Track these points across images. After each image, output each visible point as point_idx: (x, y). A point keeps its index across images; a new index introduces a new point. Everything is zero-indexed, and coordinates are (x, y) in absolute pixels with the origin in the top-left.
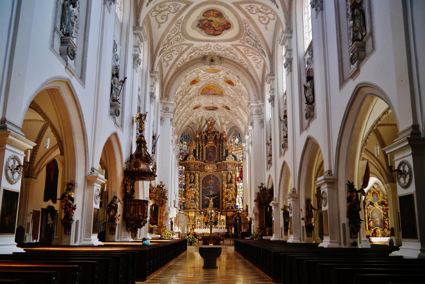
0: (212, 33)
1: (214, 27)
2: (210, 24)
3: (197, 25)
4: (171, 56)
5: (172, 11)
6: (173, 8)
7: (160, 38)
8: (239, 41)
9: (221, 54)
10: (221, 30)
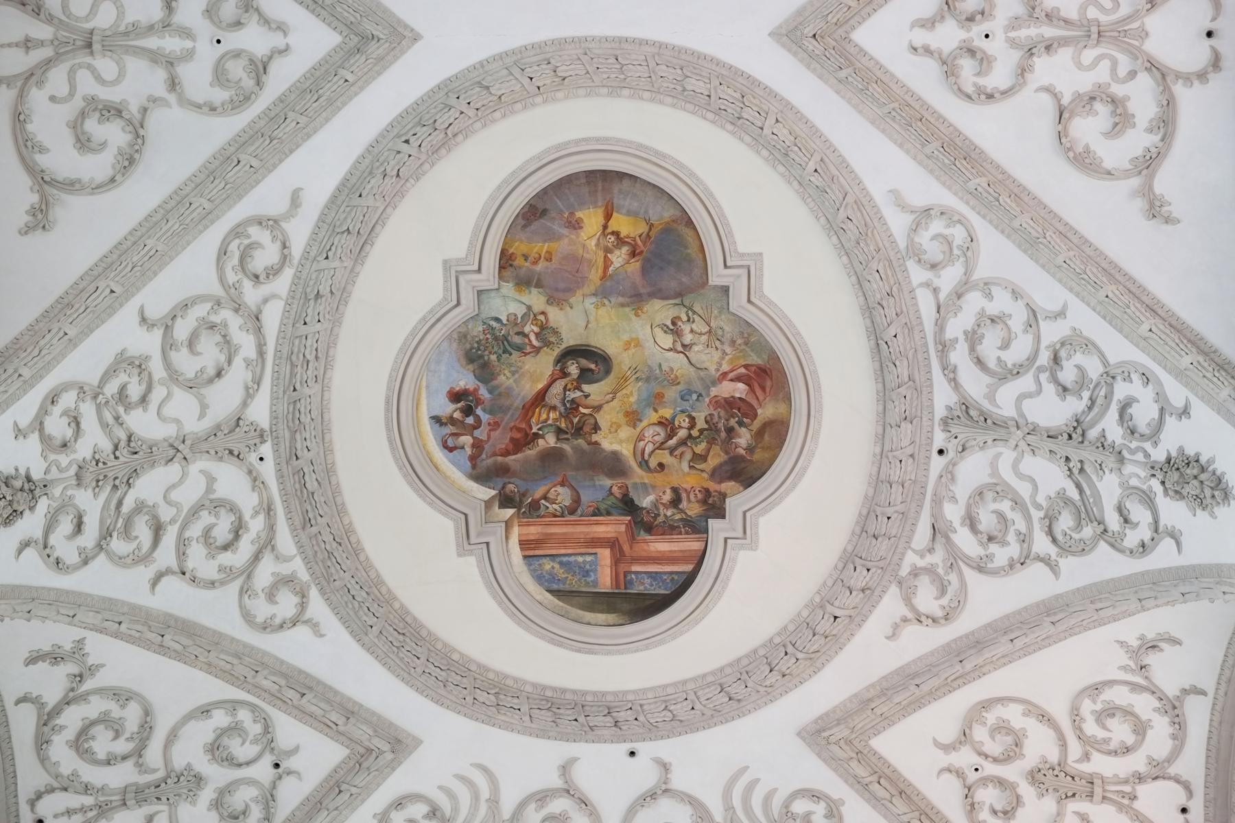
0: (604, 580)
1: (614, 465)
2: (574, 406)
6: (207, 54)
7: (23, 325)
8: (890, 605)
10: (692, 509)
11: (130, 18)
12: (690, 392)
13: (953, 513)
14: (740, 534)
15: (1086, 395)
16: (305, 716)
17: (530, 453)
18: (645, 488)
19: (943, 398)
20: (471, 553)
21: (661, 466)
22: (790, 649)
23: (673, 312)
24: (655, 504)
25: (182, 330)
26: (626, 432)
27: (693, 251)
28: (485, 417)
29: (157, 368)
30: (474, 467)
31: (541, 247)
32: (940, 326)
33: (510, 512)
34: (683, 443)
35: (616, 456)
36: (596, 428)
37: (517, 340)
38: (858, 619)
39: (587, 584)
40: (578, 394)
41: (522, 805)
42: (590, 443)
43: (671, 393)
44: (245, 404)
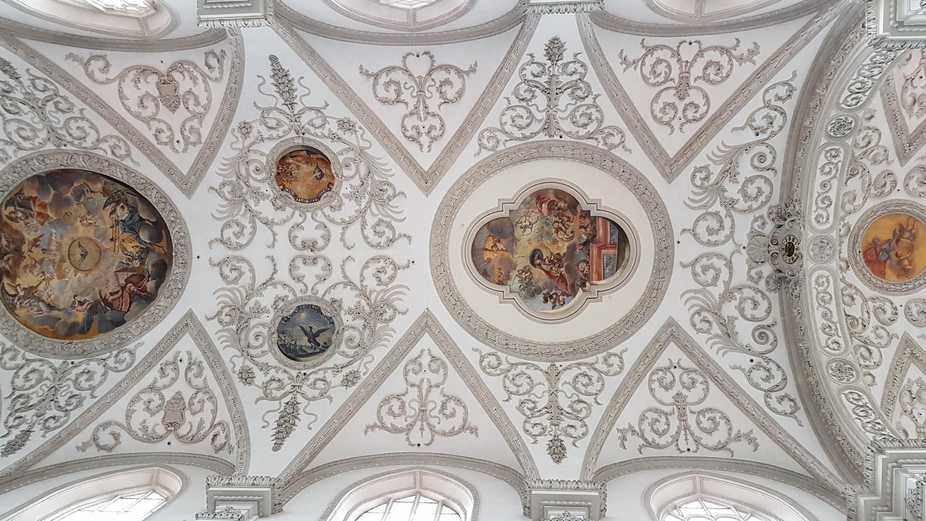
0: (613, 252)
1: (572, 248)
3: (550, 303)
4: (708, 415)
5: (436, 378)
6: (429, 375)
8: (618, 152)
9: (764, 211)
10: (588, 221)
11: (416, 398)
12: (546, 222)
13: (582, 132)
14: (595, 205)
15: (534, 89)
16: (657, 356)
17: (567, 276)
18: (580, 238)
19: (542, 137)
20: (601, 297)
21: (572, 232)
22: (636, 187)
23: (519, 228)
24: (586, 234)
25: (513, 389)
26: (560, 244)
27: (498, 222)
28: (553, 292)
29: (523, 398)
30: (571, 295)
31: (496, 272)
32: (518, 139)
33: (587, 283)
34: (564, 225)
35: (568, 248)
36: (559, 254)
37: (527, 280)
38: (625, 164)
39: (614, 258)
40: (546, 260)
41: (698, 281)
42: (564, 256)
43: (546, 229)
44: (541, 370)
